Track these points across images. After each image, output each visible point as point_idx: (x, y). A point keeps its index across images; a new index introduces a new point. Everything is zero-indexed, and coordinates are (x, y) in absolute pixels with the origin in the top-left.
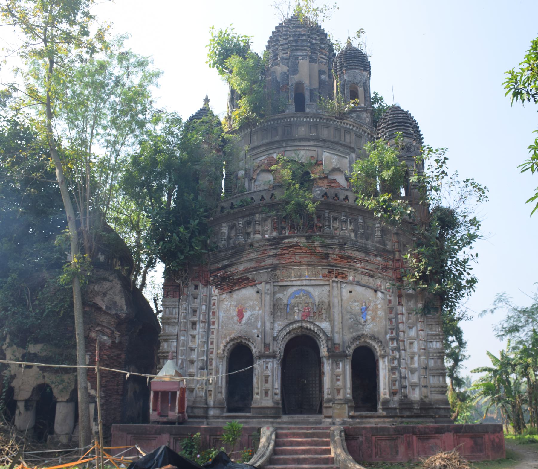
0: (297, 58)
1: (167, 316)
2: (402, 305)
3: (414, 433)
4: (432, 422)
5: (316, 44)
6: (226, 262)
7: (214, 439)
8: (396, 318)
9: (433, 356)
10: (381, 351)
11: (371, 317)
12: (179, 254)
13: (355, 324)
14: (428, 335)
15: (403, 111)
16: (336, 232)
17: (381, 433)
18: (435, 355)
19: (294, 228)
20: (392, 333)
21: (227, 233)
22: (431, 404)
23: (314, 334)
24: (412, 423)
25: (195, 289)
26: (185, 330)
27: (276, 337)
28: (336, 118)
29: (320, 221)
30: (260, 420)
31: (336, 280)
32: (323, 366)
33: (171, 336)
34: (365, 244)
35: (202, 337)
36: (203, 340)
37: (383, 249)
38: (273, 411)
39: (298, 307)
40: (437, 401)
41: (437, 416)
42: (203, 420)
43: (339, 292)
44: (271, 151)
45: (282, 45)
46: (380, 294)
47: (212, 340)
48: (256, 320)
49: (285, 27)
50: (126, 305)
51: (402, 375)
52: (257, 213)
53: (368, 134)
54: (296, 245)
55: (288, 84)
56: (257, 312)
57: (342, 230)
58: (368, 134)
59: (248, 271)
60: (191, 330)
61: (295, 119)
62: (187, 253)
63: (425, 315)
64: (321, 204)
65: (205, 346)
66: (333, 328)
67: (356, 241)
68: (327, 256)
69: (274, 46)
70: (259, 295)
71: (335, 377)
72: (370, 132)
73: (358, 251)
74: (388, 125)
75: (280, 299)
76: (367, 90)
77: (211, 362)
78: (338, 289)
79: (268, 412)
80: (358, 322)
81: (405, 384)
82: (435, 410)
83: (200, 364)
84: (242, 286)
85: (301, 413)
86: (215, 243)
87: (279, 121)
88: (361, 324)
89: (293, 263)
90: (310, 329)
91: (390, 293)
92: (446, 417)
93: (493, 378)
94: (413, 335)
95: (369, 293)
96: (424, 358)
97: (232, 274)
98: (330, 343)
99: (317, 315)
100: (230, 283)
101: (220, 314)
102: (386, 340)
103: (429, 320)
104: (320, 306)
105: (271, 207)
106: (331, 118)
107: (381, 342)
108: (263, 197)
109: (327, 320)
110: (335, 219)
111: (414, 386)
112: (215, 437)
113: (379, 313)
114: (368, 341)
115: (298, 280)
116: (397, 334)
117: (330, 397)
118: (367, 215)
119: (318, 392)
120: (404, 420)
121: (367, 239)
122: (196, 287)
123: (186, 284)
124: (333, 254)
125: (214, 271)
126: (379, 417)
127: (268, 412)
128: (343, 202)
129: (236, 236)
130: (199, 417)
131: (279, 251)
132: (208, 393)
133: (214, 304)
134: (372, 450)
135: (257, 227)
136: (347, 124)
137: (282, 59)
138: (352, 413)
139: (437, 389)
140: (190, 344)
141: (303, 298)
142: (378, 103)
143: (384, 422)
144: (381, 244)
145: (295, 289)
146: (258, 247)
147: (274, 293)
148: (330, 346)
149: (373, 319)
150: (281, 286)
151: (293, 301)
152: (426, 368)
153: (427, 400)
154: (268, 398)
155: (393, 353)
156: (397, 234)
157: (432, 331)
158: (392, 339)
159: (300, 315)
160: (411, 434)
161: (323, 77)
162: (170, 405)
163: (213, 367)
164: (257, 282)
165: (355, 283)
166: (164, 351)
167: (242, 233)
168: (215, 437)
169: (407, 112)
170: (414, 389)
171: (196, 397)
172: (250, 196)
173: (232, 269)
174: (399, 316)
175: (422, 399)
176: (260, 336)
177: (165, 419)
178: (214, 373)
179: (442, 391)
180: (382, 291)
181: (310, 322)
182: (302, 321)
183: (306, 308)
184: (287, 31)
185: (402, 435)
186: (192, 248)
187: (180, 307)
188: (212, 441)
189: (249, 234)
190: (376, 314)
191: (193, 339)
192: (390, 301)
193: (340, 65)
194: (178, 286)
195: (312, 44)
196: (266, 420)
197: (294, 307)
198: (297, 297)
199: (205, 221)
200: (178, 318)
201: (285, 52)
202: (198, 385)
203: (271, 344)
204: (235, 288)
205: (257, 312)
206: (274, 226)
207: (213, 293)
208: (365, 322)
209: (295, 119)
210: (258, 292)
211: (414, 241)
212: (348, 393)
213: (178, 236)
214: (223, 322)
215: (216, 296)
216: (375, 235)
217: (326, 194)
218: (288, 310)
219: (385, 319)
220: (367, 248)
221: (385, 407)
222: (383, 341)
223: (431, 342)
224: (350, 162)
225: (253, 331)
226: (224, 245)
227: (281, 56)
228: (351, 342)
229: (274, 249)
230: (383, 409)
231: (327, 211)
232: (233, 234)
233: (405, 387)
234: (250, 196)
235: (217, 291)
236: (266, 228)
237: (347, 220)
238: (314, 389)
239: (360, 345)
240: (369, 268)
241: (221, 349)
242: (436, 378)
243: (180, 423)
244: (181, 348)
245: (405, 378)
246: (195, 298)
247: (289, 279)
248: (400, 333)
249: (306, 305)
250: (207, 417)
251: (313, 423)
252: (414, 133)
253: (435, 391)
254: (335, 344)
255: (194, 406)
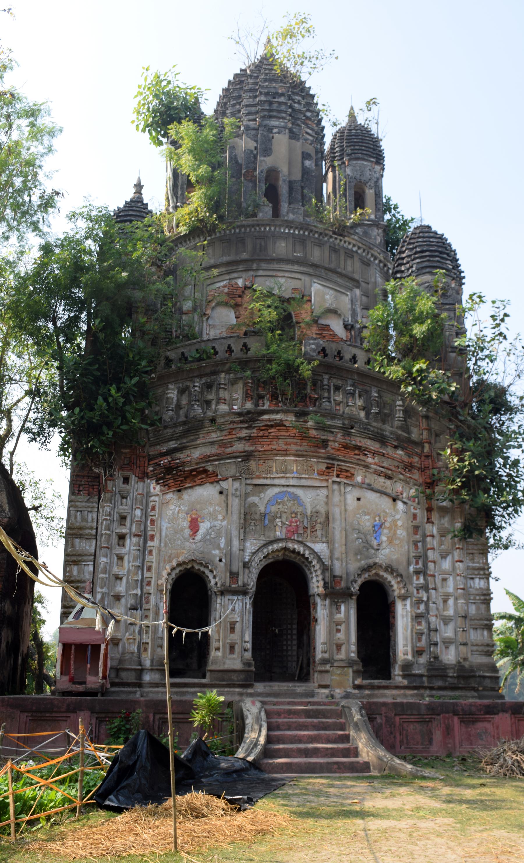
0: (270, 130)
1: (78, 524)
2: (433, 523)
3: (455, 713)
4: (473, 697)
5: (300, 111)
6: (173, 444)
7: (160, 718)
8: (424, 541)
9: (475, 599)
10: (400, 589)
11: (388, 537)
12: (105, 429)
13: (364, 547)
14: (468, 568)
15: (436, 233)
16: (338, 408)
17: (409, 712)
18: (478, 598)
19: (277, 398)
20: (417, 563)
21: (175, 399)
22: (472, 671)
23: (303, 560)
24: (448, 697)
25: (124, 483)
26: (108, 548)
27: (248, 563)
28: (334, 233)
29: (314, 390)
30: (222, 689)
31: (338, 480)
32: (315, 608)
33: (86, 555)
34: (381, 429)
35: (135, 559)
36: (137, 564)
37: (407, 438)
38: (242, 676)
39: (280, 517)
40: (481, 666)
41: (481, 689)
42: (134, 689)
43: (342, 499)
44: (235, 275)
45: (247, 106)
46: (400, 505)
47: (149, 564)
48: (218, 535)
49: (251, 76)
50: (8, 503)
51: (432, 627)
52: (222, 372)
53: (380, 261)
54: (280, 424)
55: (255, 169)
56: (220, 523)
57: (348, 406)
58: (380, 261)
59: (207, 459)
60: (117, 547)
61: (273, 228)
62: (118, 427)
63: (465, 539)
64: (319, 365)
65: (140, 573)
66: (332, 552)
67: (368, 424)
68: (325, 444)
69: (234, 105)
70: (223, 497)
71: (335, 626)
72: (382, 259)
73: (370, 438)
74: (416, 253)
75: (255, 505)
76: (378, 194)
77: (147, 598)
78: (340, 494)
79: (234, 677)
80: (368, 545)
81: (435, 640)
82: (478, 679)
83: (131, 601)
84: (198, 482)
85: (271, 679)
86: (157, 413)
87: (248, 230)
88: (373, 548)
89: (275, 452)
90: (299, 553)
91: (415, 504)
92: (493, 689)
93: (516, 630)
94: (447, 567)
95: (385, 503)
96: (463, 601)
97: (183, 464)
98: (328, 574)
99: (309, 531)
100: (179, 477)
101: (163, 523)
102: (409, 573)
103: (470, 547)
104: (314, 519)
105: (244, 364)
106: (327, 232)
107: (401, 576)
108: (229, 347)
109: (324, 539)
110: (337, 388)
111: (447, 643)
112: (161, 716)
113: (399, 532)
114: (382, 573)
115: (282, 477)
116: (425, 566)
117: (326, 656)
118: (385, 387)
119: (295, 648)
120: (434, 692)
121: (384, 422)
122: (126, 480)
123: (111, 476)
124: (334, 441)
125: (155, 457)
126: (397, 687)
127: (234, 677)
128: (349, 365)
129: (190, 405)
130: (128, 685)
131: (254, 432)
132: (142, 646)
133: (153, 508)
134: (395, 737)
135: (222, 394)
136: (349, 243)
137: (247, 128)
138: (358, 682)
139: (480, 648)
140: (116, 570)
141: (289, 505)
142: (390, 212)
143: (405, 696)
144: (404, 431)
145: (276, 490)
146: (223, 423)
147: (247, 495)
148: (327, 580)
149: (391, 541)
150: (256, 485)
151: (274, 509)
152: (465, 617)
153: (466, 664)
154: (235, 656)
155: (418, 593)
156: (427, 417)
157: (474, 563)
158: (417, 573)
159: (284, 530)
160: (451, 714)
161: (307, 163)
162: (89, 666)
163: (151, 607)
164: (219, 477)
165: (365, 486)
166: (72, 579)
167: (198, 401)
168: (161, 716)
169: (443, 235)
170: (447, 648)
171: (123, 654)
172: (210, 345)
173: (182, 456)
174: (429, 539)
175: (459, 662)
176: (224, 560)
177: (81, 688)
178: (151, 615)
179: (488, 651)
180: (405, 500)
181: (298, 542)
182: (286, 539)
183: (294, 520)
184: (256, 84)
185: (438, 715)
186: (125, 420)
187: (101, 510)
188: (157, 723)
189: (208, 403)
190: (395, 534)
191: (120, 562)
192: (415, 516)
193: (341, 151)
194: (98, 477)
195: (294, 110)
196: (232, 689)
197: (275, 517)
198: (279, 504)
199: (145, 378)
200: (97, 529)
201: (251, 117)
202: (127, 634)
203: (241, 573)
204: (187, 485)
205: (219, 522)
206: (247, 393)
207: (152, 490)
208: (379, 545)
209: (273, 228)
210: (221, 493)
211: (450, 429)
212: (351, 649)
213: (106, 400)
214: (166, 536)
215: (157, 495)
216: (394, 417)
217: (324, 350)
218: (267, 522)
219: (408, 543)
220: (383, 435)
221: (406, 673)
222: (404, 574)
223: (472, 578)
224: (352, 301)
225: (213, 552)
226: (172, 418)
227: (245, 123)
228: (359, 575)
229: (246, 428)
230: (404, 676)
231: (326, 377)
232: (184, 401)
233: (436, 644)
234: (210, 345)
235: (158, 488)
236: (235, 396)
237: (354, 391)
238: (289, 643)
239: (369, 579)
240: (385, 464)
241: (164, 579)
242: (479, 632)
243: (103, 695)
244: (101, 576)
245: (436, 630)
246: (123, 497)
247: (269, 476)
248: (430, 564)
249: (293, 515)
250: (140, 685)
251: (302, 695)
252: (453, 268)
253: (477, 651)
254: (335, 577)
255: (121, 666)
